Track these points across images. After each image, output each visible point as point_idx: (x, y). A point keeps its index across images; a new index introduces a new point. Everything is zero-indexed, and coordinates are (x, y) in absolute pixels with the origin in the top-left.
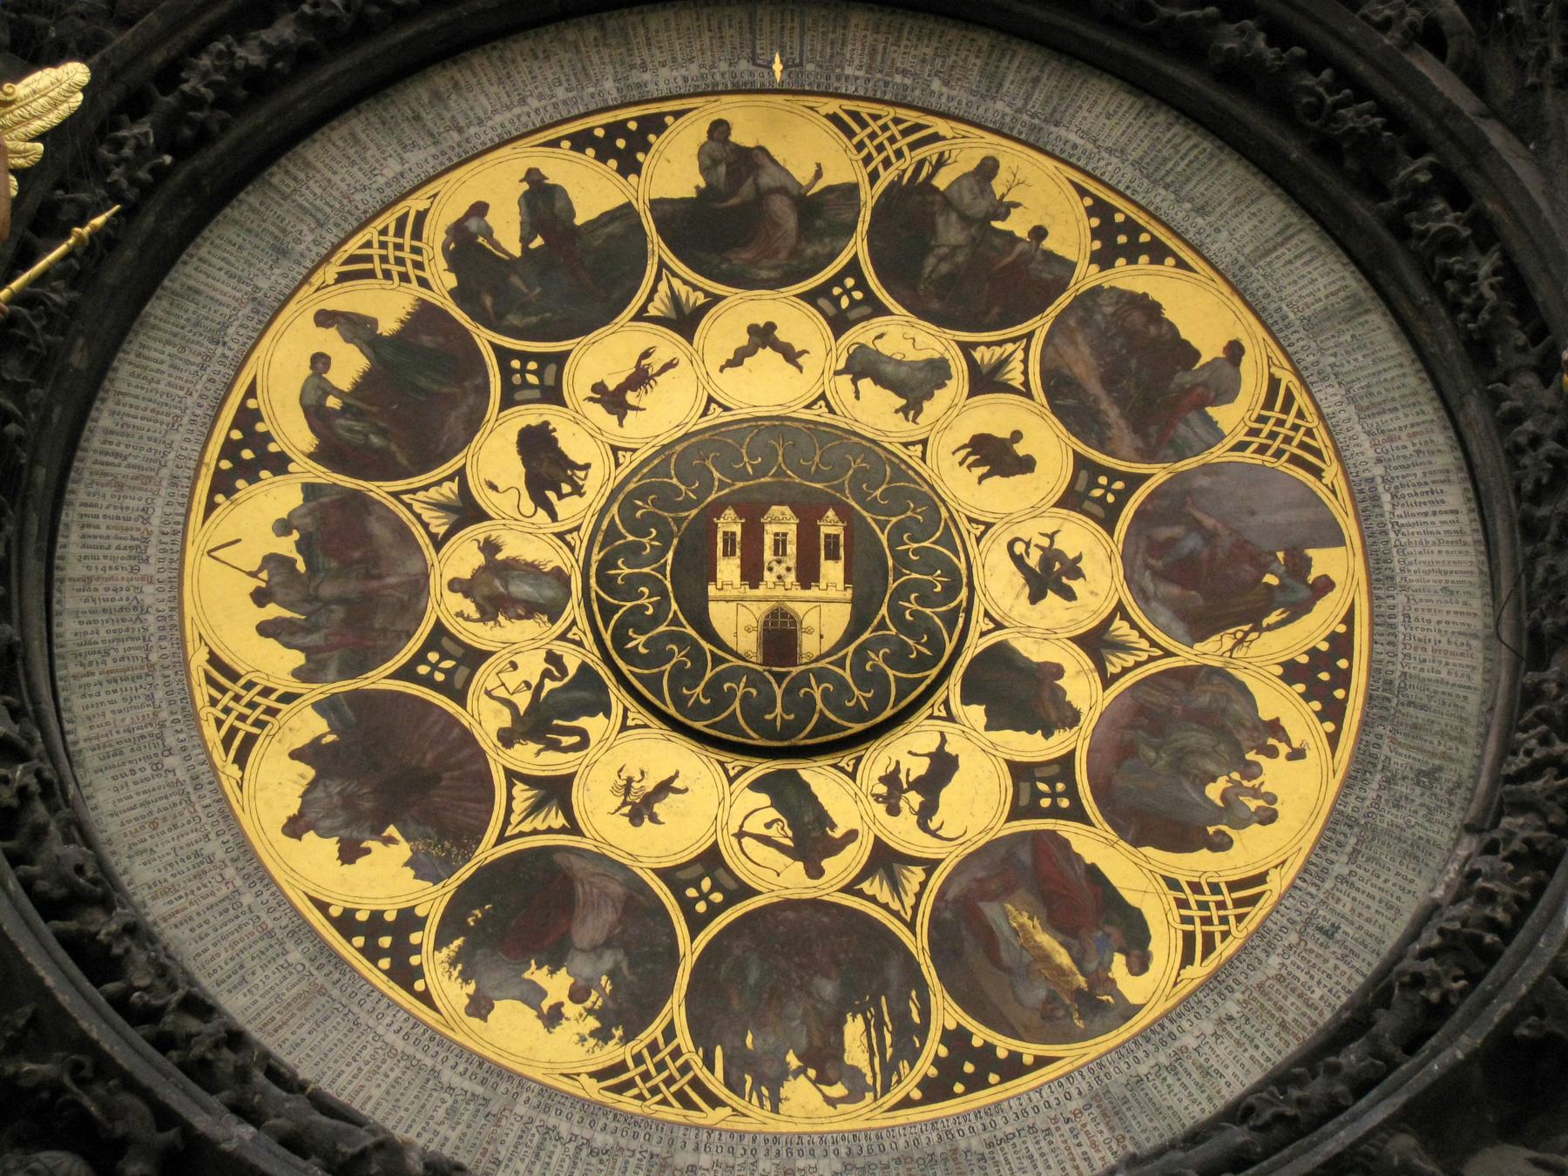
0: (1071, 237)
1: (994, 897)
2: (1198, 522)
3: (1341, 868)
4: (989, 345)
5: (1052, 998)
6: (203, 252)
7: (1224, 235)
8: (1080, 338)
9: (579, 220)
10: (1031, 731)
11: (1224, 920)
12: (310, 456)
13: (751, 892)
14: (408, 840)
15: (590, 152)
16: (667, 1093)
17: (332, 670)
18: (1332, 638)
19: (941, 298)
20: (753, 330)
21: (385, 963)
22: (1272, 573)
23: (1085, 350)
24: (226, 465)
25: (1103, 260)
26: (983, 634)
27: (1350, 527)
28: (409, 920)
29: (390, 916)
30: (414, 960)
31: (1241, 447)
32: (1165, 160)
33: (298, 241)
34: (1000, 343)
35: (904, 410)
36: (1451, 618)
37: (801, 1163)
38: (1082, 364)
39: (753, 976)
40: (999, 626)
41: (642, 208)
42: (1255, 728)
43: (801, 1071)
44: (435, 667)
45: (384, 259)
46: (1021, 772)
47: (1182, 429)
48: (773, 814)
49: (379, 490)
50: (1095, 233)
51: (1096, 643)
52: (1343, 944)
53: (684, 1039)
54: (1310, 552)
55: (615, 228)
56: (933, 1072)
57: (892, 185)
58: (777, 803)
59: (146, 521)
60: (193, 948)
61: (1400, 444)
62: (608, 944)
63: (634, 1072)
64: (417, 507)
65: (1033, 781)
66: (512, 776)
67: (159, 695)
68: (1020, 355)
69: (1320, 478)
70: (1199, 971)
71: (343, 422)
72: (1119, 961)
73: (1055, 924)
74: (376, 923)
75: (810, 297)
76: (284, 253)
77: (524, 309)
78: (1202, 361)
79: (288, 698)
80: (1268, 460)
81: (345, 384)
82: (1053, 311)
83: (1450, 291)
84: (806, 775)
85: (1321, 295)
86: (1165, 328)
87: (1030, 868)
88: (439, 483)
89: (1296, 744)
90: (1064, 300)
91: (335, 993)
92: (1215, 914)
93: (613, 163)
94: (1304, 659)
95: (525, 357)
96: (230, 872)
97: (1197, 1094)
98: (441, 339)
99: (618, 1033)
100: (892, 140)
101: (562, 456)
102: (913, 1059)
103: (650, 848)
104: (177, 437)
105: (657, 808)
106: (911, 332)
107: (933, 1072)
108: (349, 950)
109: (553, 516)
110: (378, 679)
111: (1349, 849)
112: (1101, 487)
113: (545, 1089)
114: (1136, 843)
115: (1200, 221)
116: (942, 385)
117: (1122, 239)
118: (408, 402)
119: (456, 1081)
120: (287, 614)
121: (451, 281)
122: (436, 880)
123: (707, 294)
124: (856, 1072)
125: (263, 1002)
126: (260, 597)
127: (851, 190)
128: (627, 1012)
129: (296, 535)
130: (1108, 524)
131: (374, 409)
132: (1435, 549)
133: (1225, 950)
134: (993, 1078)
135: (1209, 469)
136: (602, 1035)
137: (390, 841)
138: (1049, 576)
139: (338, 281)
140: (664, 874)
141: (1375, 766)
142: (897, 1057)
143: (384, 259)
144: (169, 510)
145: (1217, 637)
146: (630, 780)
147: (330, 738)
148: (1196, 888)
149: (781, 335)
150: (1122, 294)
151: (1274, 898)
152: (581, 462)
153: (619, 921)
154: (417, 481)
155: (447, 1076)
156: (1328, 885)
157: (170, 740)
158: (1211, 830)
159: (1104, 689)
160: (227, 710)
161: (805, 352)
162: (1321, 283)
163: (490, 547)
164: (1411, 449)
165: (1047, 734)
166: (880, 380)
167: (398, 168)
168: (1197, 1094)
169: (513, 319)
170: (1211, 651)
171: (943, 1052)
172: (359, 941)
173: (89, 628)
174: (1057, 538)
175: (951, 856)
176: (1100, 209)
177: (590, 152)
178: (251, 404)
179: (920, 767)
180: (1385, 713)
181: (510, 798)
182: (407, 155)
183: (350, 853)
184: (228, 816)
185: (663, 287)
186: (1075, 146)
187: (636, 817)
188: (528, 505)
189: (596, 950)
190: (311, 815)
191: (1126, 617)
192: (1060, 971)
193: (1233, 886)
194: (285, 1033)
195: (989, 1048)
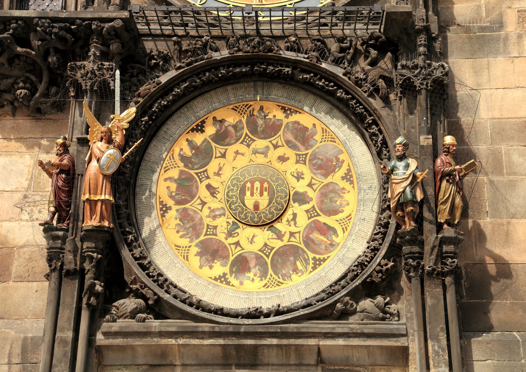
1: (311, 234)
3: (362, 208)
5: (326, 246)
6: (140, 177)
9: (198, 145)
11: (347, 224)
13: (273, 248)
16: (275, 285)
17: (194, 239)
18: (347, 170)
20: (235, 153)
21: (224, 283)
23: (290, 134)
25: (287, 117)
27: (343, 149)
28: (225, 274)
29: (222, 275)
30: (228, 280)
31: (321, 142)
35: (265, 157)
37: (299, 288)
38: (290, 137)
39: (280, 261)
40: (294, 188)
45: (170, 165)
46: (307, 211)
47: (311, 142)
48: (272, 234)
49: (187, 206)
51: (310, 185)
53: (274, 275)
55: (205, 143)
56: (313, 265)
58: (272, 232)
62: (256, 265)
63: (269, 284)
65: (309, 212)
66: (229, 244)
67: (170, 255)
72: (334, 236)
74: (220, 277)
75: (242, 143)
77: (196, 164)
79: (190, 247)
80: (326, 142)
81: (175, 190)
92: (345, 223)
95: (200, 173)
96: (194, 279)
99: (263, 279)
100: (244, 109)
105: (254, 240)
107: (313, 265)
108: (218, 283)
109: (217, 198)
113: (257, 292)
114: (329, 216)
117: (289, 112)
118: (185, 189)
119: (244, 297)
121: (183, 164)
122: (226, 266)
124: (301, 270)
126: (178, 232)
128: (264, 274)
130: (305, 164)
134: (322, 263)
135: (318, 148)
136: (261, 280)
137: (216, 263)
138: (299, 177)
140: (260, 250)
142: (306, 265)
143: (170, 165)
148: (341, 220)
150: (292, 122)
155: (242, 296)
157: (175, 262)
163: (209, 208)
165: (309, 203)
166: (259, 153)
169: (196, 167)
170: (329, 179)
171: (313, 262)
172: (219, 281)
175: (302, 229)
178: (161, 200)
179: (291, 217)
183: (211, 267)
185: (217, 151)
187: (251, 243)
188: (212, 198)
189: (255, 267)
191: (314, 179)
192: (326, 242)
193: (347, 218)
194: (215, 300)
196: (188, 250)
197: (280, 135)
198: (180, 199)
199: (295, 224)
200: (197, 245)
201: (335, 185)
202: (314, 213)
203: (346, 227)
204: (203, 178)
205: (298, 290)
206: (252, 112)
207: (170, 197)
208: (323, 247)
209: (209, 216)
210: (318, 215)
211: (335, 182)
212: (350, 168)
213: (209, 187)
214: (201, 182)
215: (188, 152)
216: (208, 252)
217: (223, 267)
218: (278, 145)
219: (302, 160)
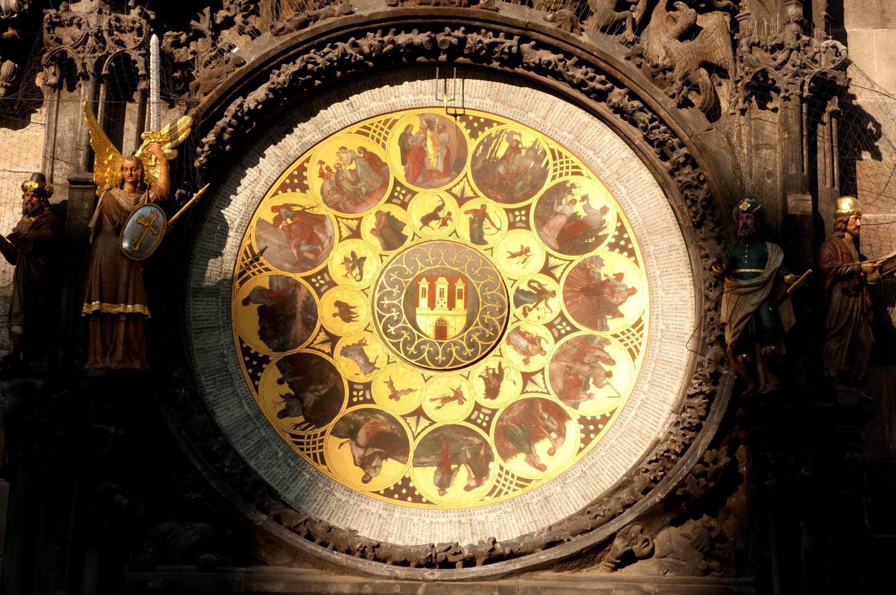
0: (271, 374)
3: (334, 121)
4: (323, 352)
5: (440, 132)
7: (221, 343)
8: (292, 337)
9: (435, 468)
10: (393, 217)
11: (377, 126)
12: (570, 419)
14: (600, 274)
15: (417, 493)
16: (564, 160)
18: (285, 191)
19: (328, 377)
20: (398, 399)
21: (626, 236)
23: (293, 332)
24: (600, 426)
25: (266, 359)
28: (612, 247)
29: (617, 250)
30: (617, 233)
31: (267, 269)
32: (220, 381)
33: (539, 501)
34: (319, 350)
35: (365, 344)
37: (539, 120)
39: (520, 184)
43: (523, 148)
44: (564, 328)
46: (404, 206)
47: (281, 287)
48: (485, 231)
49: (553, 397)
50: (262, 370)
51: (356, 234)
53: (551, 174)
55: (423, 460)
56: (486, 128)
57: (318, 427)
59: (636, 415)
60: (681, 263)
62: (557, 214)
64: (543, 386)
66: (558, 281)
67: (657, 351)
70: (394, 116)
71: (554, 427)
72: (413, 133)
74: (623, 249)
75: (371, 401)
76: (546, 498)
77: (471, 444)
78: (258, 305)
79: (616, 336)
81: (546, 440)
82: (294, 351)
84: (469, 239)
85: (205, 303)
88: (532, 392)
89: (319, 166)
91: (645, 231)
92: (378, 130)
93: (411, 485)
94: (298, 190)
95: (480, 426)
96: (660, 283)
98: (506, 444)
99: (568, 185)
100: (308, 444)
101: (486, 384)
102: (489, 136)
104: (614, 442)
105: (518, 250)
106: (346, 371)
107: (486, 128)
108: (634, 245)
109: (500, 364)
114: (385, 164)
116: (347, 346)
118: (528, 425)
119: (623, 189)
120: (603, 365)
121: (491, 465)
122: (597, 257)
123: (405, 420)
124: (508, 140)
125: (668, 237)
126: (609, 374)
127: (333, 433)
128: (561, 190)
129: (588, 392)
130: (326, 270)
133: (383, 118)
135: (282, 269)
136: (573, 186)
137: (605, 276)
139: (531, 480)
140: (528, 227)
142: (494, 139)
147: (608, 317)
148: (378, 141)
149: (390, 393)
152: (481, 379)
156: (341, 118)
157: (660, 334)
158: (362, 155)
162: (201, 307)
163: (526, 362)
165: (389, 213)
166: (366, 359)
167: (490, 515)
169: (477, 441)
170: (323, 210)
171: (480, 133)
172: (630, 246)
175: (441, 191)
176: (254, 378)
177: (417, 493)
178: (582, 445)
179: (433, 223)
181: (562, 274)
182: (484, 519)
183: (619, 276)
184: (652, 302)
185: (419, 430)
186: (248, 404)
187: (527, 250)
188: (506, 371)
189: (561, 213)
190: (626, 293)
192: (432, 139)
193: (367, 135)
194: (665, 225)
195: (467, 127)
196: (623, 333)
198: (552, 419)
199: (440, 208)
200: (605, 328)
202: (400, 192)
203: (385, 124)
204: (485, 415)
205: (544, 118)
206: (303, 426)
207: (564, 436)
209: (541, 351)
210: (397, 183)
211: (320, 197)
212: (278, 190)
213: (492, 392)
214: (494, 411)
215: (463, 475)
216: (598, 302)
217: (602, 260)
218: (326, 337)
219: (323, 278)
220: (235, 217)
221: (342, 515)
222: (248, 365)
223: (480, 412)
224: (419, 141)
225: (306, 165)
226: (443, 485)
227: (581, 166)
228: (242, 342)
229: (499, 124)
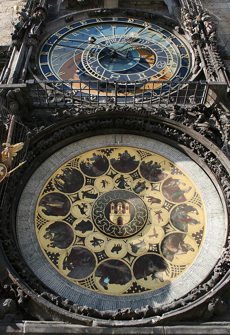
0: (141, 282)
2: (87, 263)
4: (133, 260)
5: (48, 200)
7: (125, 302)
8: (126, 272)
11: (39, 222)
14: (117, 160)
16: (72, 163)
22: (72, 265)
23: (123, 271)
25: (135, 284)
26: (95, 229)
31: (92, 277)
34: (133, 261)
36: (45, 278)
38: (121, 269)
40: (94, 231)
41: (185, 233)
42: (56, 245)
43: (63, 175)
46: (75, 219)
48: (92, 193)
50: (140, 286)
51: (83, 239)
52: (24, 229)
54: (70, 271)
56: (52, 185)
61: (73, 295)
62: (91, 169)
68: (129, 262)
69: (78, 281)
70: (37, 214)
71: (174, 182)
72: (46, 210)
73: (55, 207)
74: (110, 152)
79: (142, 159)
80: (87, 278)
82: (132, 272)
83: (16, 130)
86: (117, 283)
87: (64, 210)
88: (160, 188)
90: (133, 274)
92: (40, 222)
94: (58, 257)
95: (171, 207)
96: (125, 143)
97: (25, 203)
98: (180, 199)
99: (81, 164)
103: (98, 181)
105: (103, 184)
108: (109, 148)
110: (138, 168)
111: (32, 239)
112: (102, 257)
115: (130, 300)
119: (88, 147)
120: (152, 165)
128: (83, 166)
130: (96, 253)
131: (174, 187)
132: (55, 285)
133: (36, 219)
136: (82, 162)
137: (118, 159)
138: (95, 242)
139: (195, 192)
141: (38, 251)
143: (196, 199)
144: (172, 159)
145: (70, 252)
146: (108, 183)
148: (45, 223)
150: (127, 282)
151: (36, 228)
153: (93, 172)
154: (161, 186)
156: (31, 234)
158: (49, 230)
159: (76, 235)
160: (144, 153)
161: (150, 238)
164: (71, 296)
168: (25, 203)
169: (178, 208)
170: (69, 249)
173: (162, 146)
174: (100, 247)
176: (143, 290)
179: (85, 210)
180: (42, 258)
183: (120, 154)
186: (156, 293)
187: (103, 181)
189: (92, 168)
191: (82, 245)
193: (41, 226)
195: (49, 191)
197: (131, 266)
198: (171, 183)
199: (79, 207)
201: (62, 247)
202: (69, 220)
204: (167, 205)
206: (167, 272)
208: (50, 200)
210: (65, 220)
211: (63, 249)
213: (158, 201)
214: (166, 201)
215: (191, 215)
220: (64, 285)
221: (209, 261)
222: (137, 291)
223: (166, 206)
224: (49, 208)
225: (47, 252)
226: (196, 222)
227: (76, 158)
228: (125, 293)
229: (51, 180)
